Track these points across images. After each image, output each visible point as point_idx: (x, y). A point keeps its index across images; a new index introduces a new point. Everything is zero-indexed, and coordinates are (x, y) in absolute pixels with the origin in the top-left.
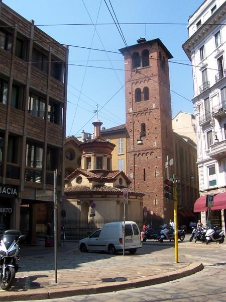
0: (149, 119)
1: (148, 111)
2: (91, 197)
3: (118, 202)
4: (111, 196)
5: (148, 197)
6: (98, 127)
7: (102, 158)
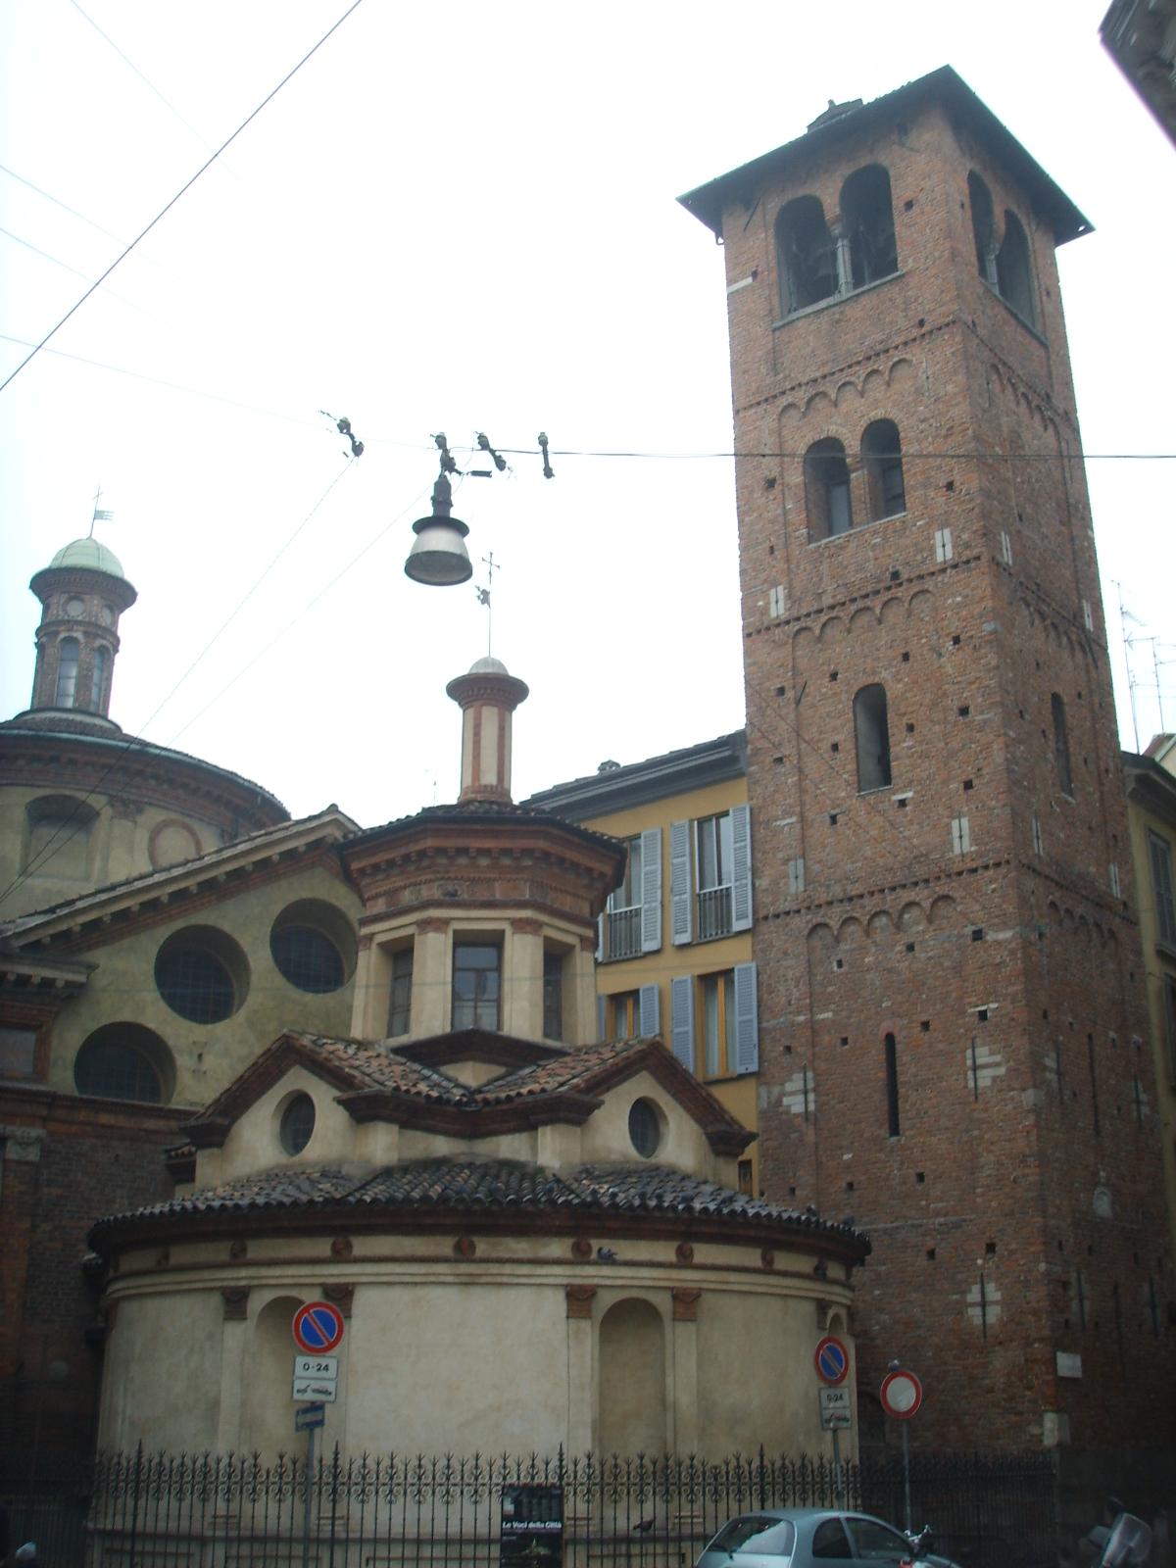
0: (913, 649)
1: (899, 592)
2: (341, 1255)
3: (579, 1299)
4: (520, 1247)
5: (923, 1261)
6: (490, 714)
7: (496, 941)
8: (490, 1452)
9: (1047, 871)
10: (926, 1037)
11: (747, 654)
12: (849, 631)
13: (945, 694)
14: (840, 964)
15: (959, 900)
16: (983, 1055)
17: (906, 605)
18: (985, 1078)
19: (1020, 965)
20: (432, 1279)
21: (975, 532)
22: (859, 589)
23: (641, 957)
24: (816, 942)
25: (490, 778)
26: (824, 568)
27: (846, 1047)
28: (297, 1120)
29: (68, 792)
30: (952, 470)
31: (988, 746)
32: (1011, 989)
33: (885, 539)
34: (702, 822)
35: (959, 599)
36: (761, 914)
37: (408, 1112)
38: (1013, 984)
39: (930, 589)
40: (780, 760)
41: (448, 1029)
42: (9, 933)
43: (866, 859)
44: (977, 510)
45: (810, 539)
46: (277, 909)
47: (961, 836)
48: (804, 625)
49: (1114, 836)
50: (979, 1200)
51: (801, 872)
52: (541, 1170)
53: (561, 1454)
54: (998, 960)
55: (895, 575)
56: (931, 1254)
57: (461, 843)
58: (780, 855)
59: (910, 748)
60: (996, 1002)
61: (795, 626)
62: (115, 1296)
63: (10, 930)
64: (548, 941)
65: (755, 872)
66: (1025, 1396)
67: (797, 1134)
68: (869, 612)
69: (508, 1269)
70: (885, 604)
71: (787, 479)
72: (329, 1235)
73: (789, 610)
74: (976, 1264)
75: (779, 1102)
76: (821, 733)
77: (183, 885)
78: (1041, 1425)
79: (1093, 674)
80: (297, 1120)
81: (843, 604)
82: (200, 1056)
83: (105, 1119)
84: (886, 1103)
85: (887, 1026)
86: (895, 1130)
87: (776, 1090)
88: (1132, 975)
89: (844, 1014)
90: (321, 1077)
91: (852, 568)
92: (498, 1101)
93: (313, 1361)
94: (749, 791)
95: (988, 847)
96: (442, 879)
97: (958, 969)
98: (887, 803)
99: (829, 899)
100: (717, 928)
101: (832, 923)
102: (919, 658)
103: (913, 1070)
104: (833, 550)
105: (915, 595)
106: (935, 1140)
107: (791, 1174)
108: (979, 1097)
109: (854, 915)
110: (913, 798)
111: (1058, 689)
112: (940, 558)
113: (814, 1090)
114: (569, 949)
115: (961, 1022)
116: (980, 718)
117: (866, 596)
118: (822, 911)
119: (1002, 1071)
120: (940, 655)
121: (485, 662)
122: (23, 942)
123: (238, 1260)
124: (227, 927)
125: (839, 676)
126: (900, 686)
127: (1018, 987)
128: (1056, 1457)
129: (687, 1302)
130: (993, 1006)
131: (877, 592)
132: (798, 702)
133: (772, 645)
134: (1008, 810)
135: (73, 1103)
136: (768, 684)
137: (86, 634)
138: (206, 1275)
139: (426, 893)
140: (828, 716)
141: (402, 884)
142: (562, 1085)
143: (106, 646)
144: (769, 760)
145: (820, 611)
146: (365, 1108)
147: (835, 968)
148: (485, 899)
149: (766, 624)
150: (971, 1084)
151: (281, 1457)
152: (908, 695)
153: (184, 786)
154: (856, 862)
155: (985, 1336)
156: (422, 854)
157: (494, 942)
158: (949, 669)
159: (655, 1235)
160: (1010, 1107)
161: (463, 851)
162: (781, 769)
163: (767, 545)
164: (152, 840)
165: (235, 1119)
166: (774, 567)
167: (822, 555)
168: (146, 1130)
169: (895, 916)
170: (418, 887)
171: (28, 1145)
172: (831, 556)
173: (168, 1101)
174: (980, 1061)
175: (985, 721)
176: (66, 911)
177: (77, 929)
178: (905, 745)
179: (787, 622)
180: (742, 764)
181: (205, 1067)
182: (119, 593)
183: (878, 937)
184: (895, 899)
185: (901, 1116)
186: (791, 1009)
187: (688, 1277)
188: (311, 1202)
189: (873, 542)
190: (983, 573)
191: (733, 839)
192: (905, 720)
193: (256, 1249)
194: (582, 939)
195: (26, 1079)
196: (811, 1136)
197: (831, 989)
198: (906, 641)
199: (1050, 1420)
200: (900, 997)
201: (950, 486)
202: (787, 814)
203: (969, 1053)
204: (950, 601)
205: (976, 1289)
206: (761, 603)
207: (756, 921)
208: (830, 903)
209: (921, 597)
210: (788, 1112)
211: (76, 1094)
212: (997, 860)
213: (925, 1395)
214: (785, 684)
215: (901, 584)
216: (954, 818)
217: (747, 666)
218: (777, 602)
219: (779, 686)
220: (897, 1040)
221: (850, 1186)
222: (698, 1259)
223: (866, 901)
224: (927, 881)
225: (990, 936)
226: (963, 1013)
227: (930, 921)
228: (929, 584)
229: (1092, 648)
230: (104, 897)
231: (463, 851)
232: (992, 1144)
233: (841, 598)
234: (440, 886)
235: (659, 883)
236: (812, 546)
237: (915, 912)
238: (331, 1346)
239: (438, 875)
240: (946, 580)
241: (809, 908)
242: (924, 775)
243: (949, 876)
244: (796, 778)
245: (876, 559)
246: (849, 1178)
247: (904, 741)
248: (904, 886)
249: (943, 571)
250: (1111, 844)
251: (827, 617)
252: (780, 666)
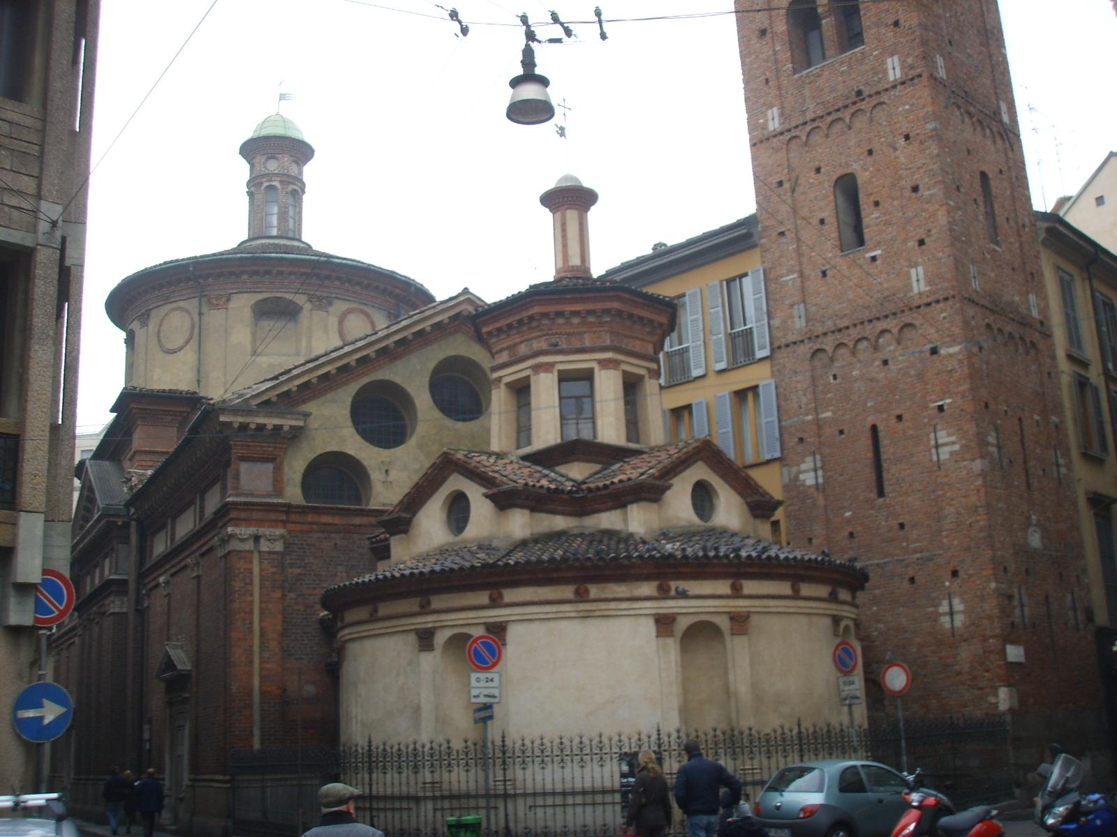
0: (875, 146)
1: (863, 105)
2: (496, 602)
3: (664, 623)
4: (621, 590)
5: (906, 585)
6: (572, 215)
7: (588, 376)
8: (609, 731)
9: (982, 301)
10: (900, 426)
11: (754, 159)
12: (827, 136)
13: (901, 178)
14: (835, 377)
15: (918, 326)
16: (943, 437)
17: (868, 114)
18: (945, 453)
19: (966, 370)
20: (560, 615)
21: (917, 57)
22: (833, 105)
23: (690, 382)
24: (817, 363)
25: (575, 261)
26: (806, 92)
27: (843, 436)
28: (458, 510)
29: (279, 295)
30: (897, 12)
31: (934, 214)
32: (961, 388)
33: (850, 67)
34: (729, 281)
35: (907, 107)
36: (776, 344)
37: (536, 501)
38: (961, 385)
39: (886, 101)
40: (782, 234)
41: (559, 441)
42: (248, 396)
43: (849, 300)
44: (917, 40)
45: (795, 71)
46: (432, 365)
47: (918, 282)
48: (794, 134)
49: (1032, 274)
50: (945, 540)
51: (803, 312)
52: (631, 535)
53: (659, 731)
54: (950, 368)
55: (859, 93)
56: (912, 580)
58: (787, 302)
59: (876, 218)
60: (950, 398)
61: (788, 136)
62: (343, 639)
63: (247, 394)
64: (625, 373)
65: (770, 315)
66: (984, 677)
67: (810, 500)
68: (841, 122)
69: (613, 605)
70: (853, 115)
71: (775, 29)
72: (485, 590)
73: (784, 123)
74: (944, 586)
75: (797, 478)
76: (811, 212)
77: (365, 353)
78: (996, 695)
79: (1011, 155)
80: (458, 510)
81: (822, 117)
82: (387, 471)
83: (325, 519)
84: (874, 474)
85: (871, 420)
86: (881, 493)
87: (794, 470)
88: (1049, 374)
89: (840, 413)
90: (472, 480)
91: (826, 90)
92: (598, 488)
93: (482, 676)
94: (762, 257)
95: (939, 287)
96: (547, 334)
97: (921, 376)
98: (862, 260)
99: (825, 331)
100: (745, 356)
101: (827, 348)
102: (880, 152)
103: (892, 450)
104: (812, 78)
105: (875, 107)
106: (910, 499)
107: (808, 529)
108: (942, 467)
109: (844, 341)
110: (881, 255)
111: (984, 168)
112: (891, 78)
113: (822, 468)
114: (640, 379)
115: (925, 414)
116: (927, 193)
117: (838, 110)
118: (820, 340)
119: (957, 447)
120: (895, 149)
121: (566, 178)
122: (259, 401)
123: (425, 610)
124: (398, 380)
125: (822, 170)
126: (867, 173)
127: (965, 387)
128: (1008, 718)
129: (740, 622)
130: (948, 401)
131: (846, 107)
132: (793, 191)
133: (771, 150)
134: (951, 258)
135: (302, 510)
136: (770, 179)
137: (281, 182)
138: (404, 621)
139: (537, 345)
140: (816, 199)
141: (519, 340)
142: (642, 474)
143: (295, 189)
144: (775, 234)
145: (805, 123)
146: (504, 500)
147: (832, 381)
148: (579, 346)
149: (766, 136)
150: (935, 458)
151: (466, 742)
152: (874, 180)
153: (359, 283)
154: (844, 302)
156: (531, 318)
157: (587, 376)
158: (903, 159)
159: (715, 576)
160: (964, 473)
161: (560, 314)
162: (784, 240)
163: (763, 78)
164: (341, 323)
165: (414, 513)
166: (769, 93)
167: (804, 82)
168: (353, 525)
169: (873, 340)
170: (530, 342)
171: (275, 540)
172: (810, 83)
173: (367, 504)
174: (940, 441)
175: (931, 195)
176: (285, 377)
177: (295, 389)
178: (874, 216)
179: (782, 133)
180: (755, 238)
181: (390, 479)
182: (301, 151)
183: (861, 356)
184: (874, 328)
185: (886, 483)
186: (802, 411)
187: (740, 605)
188: (473, 567)
189: (841, 70)
190: (925, 86)
191: (751, 289)
192: (872, 199)
193: (437, 602)
194: (649, 370)
195: (269, 496)
196: (821, 501)
197: (829, 395)
198: (870, 141)
199: (1003, 693)
200: (880, 399)
201: (896, 24)
202: (790, 272)
203: (932, 435)
204: (901, 109)
205: (945, 603)
206: (761, 121)
207: (772, 350)
208: (825, 334)
209: (879, 108)
210: (803, 485)
211: (304, 503)
212: (946, 296)
213: (913, 679)
214: (783, 178)
215: (863, 100)
216: (912, 267)
217: (754, 167)
218: (773, 119)
219: (778, 180)
220: (879, 429)
221: (851, 535)
222: (746, 591)
223: (851, 331)
224: (894, 314)
225: (943, 352)
226: (926, 407)
227: (899, 343)
228: (884, 98)
229: (1008, 136)
230: (311, 365)
231: (560, 314)
232: (952, 499)
233: (819, 113)
234: (547, 339)
235: (701, 327)
236: (796, 76)
237: (887, 336)
238: (495, 665)
239: (545, 332)
240: (897, 94)
241: (810, 339)
242: (889, 237)
243: (911, 309)
244: (795, 246)
245: (844, 82)
246: (850, 529)
247: (873, 214)
248: (878, 319)
249: (894, 87)
250: (1029, 279)
251: (810, 127)
252: (779, 166)
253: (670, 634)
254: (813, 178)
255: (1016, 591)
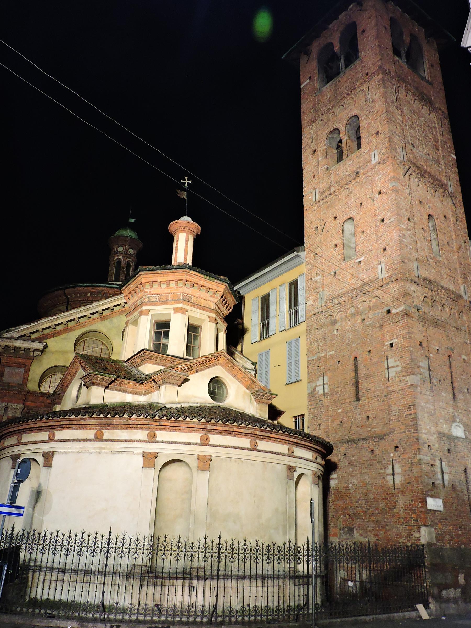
2: (51, 440)
53: (110, 532)
57: (154, 279)
69: (116, 444)
74: (390, 456)
75: (315, 389)
85: (354, 354)
108: (391, 381)
119: (399, 369)
124: (104, 330)
130: (396, 340)
137: (123, 256)
155: (394, 489)
174: (389, 366)
178: (361, 239)
187: (206, 451)
197: (334, 342)
203: (386, 361)
205: (390, 467)
210: (317, 393)
225: (394, 311)
253: (153, 466)
254: (333, 223)
255: (438, 463)
